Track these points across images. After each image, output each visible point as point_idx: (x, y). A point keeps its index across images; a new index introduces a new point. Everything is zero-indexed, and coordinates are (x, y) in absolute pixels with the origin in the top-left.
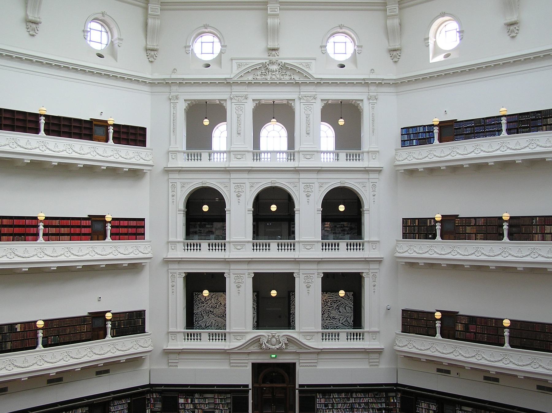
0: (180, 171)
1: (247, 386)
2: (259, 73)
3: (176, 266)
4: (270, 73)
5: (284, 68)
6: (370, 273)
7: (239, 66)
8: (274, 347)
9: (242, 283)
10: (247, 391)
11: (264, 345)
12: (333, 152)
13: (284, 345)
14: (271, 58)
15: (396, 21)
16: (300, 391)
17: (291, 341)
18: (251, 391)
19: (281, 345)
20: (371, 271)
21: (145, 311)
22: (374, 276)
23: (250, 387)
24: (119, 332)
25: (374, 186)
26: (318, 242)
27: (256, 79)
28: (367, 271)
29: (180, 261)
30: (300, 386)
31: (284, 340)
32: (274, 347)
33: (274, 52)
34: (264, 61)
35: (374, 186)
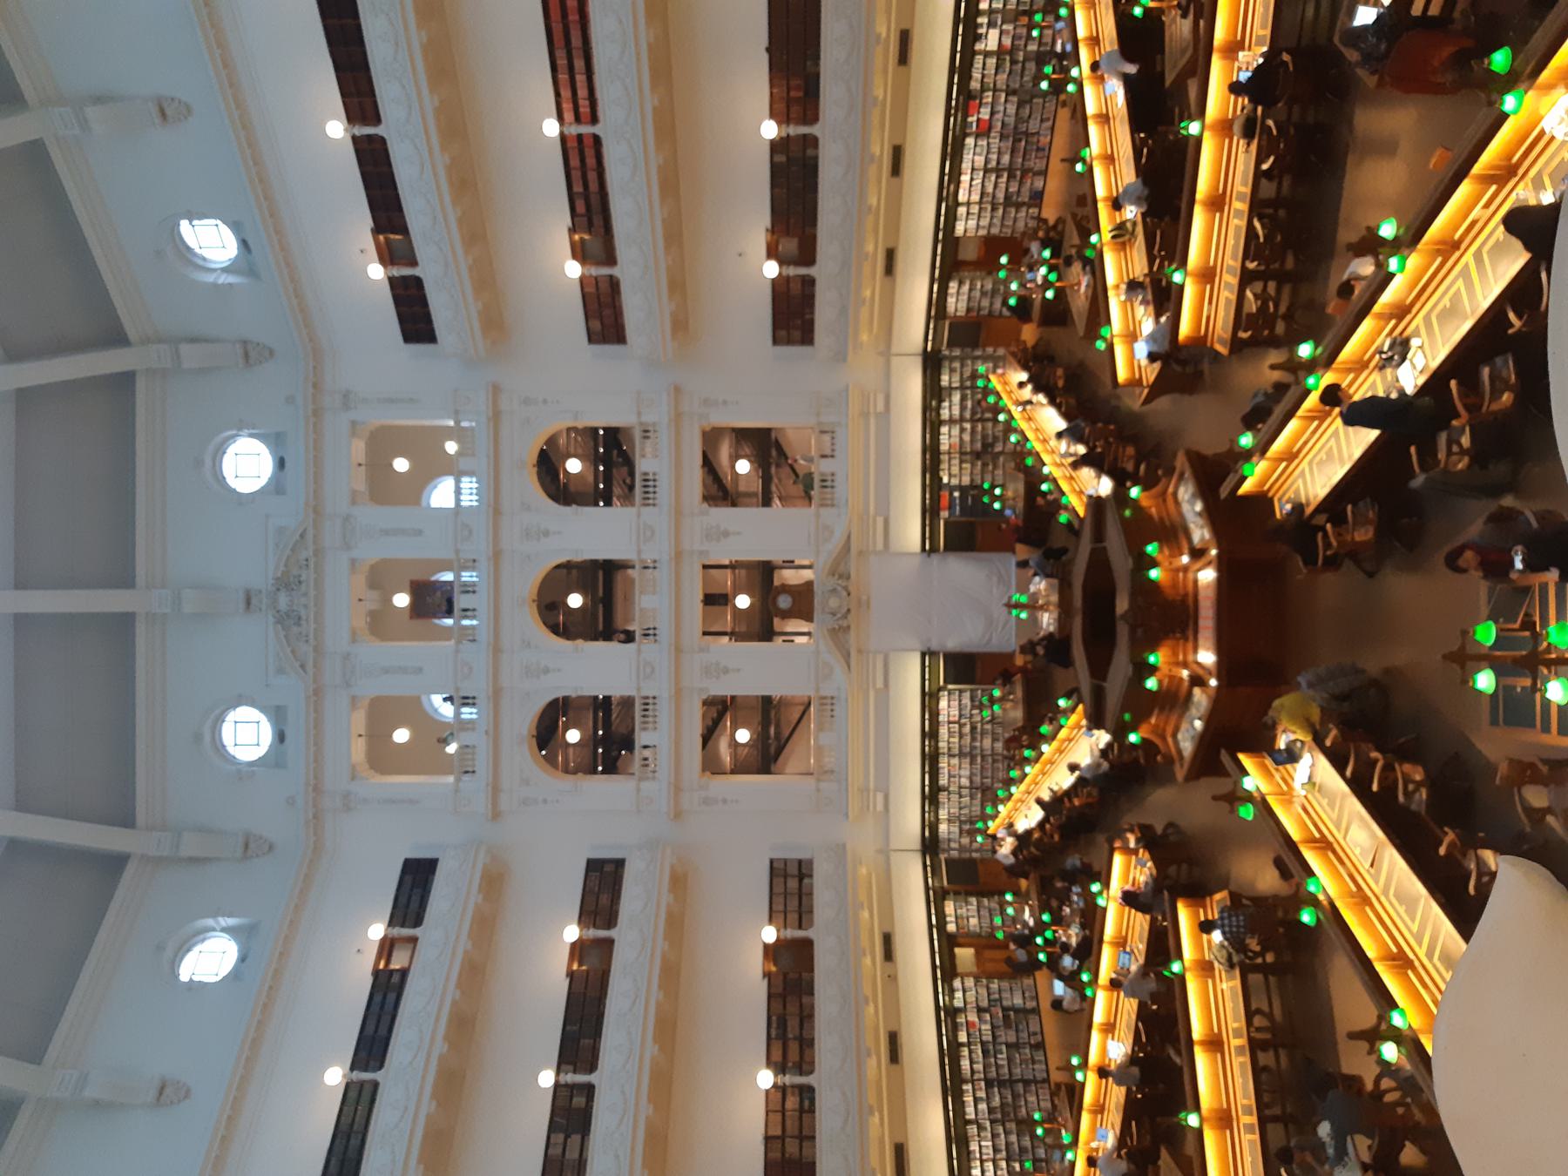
0: (496, 789)
2: (295, 629)
4: (295, 608)
5: (286, 583)
7: (280, 671)
11: (840, 622)
12: (458, 482)
14: (264, 607)
15: (185, 349)
19: (839, 588)
25: (527, 401)
26: (639, 515)
27: (307, 636)
29: (677, 788)
33: (254, 601)
34: (271, 620)
35: (527, 401)
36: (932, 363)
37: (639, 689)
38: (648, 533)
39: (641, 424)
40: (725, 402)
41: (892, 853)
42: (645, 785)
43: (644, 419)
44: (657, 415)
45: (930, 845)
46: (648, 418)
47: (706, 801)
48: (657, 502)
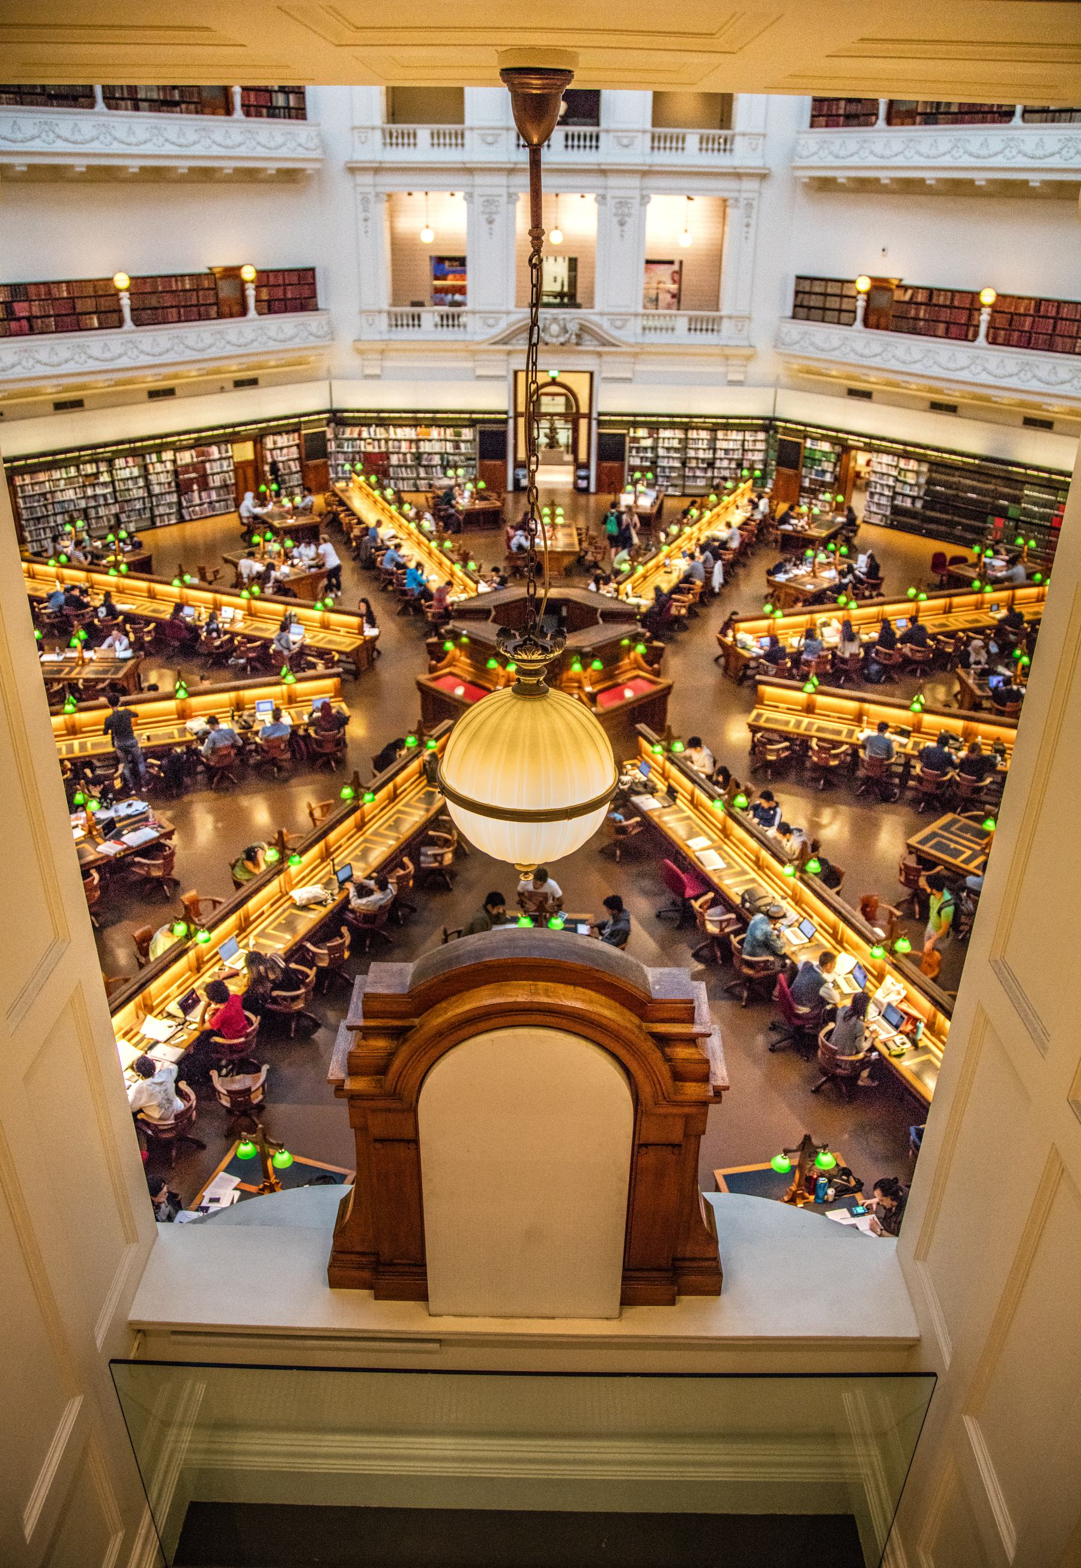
1: (506, 413)
3: (367, 179)
6: (741, 199)
8: (554, 340)
9: (496, 213)
10: (505, 422)
13: (574, 337)
16: (600, 424)
17: (584, 330)
18: (511, 422)
19: (567, 336)
20: (744, 195)
21: (313, 270)
22: (749, 206)
23: (511, 414)
24: (270, 307)
26: (644, 132)
28: (736, 194)
30: (600, 414)
31: (573, 327)
32: (554, 340)
36: (769, 425)
37: (472, 129)
38: (625, 141)
39: (733, 136)
40: (748, 225)
41: (327, 383)
42: (378, 135)
43: (738, 140)
44: (742, 155)
45: (337, 418)
46: (740, 144)
47: (365, 200)
48: (656, 150)
